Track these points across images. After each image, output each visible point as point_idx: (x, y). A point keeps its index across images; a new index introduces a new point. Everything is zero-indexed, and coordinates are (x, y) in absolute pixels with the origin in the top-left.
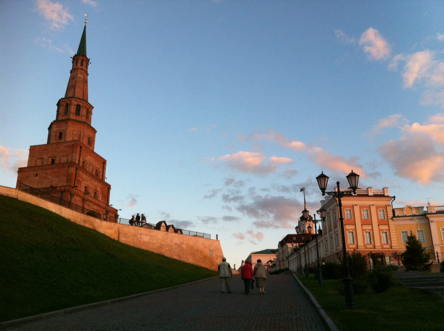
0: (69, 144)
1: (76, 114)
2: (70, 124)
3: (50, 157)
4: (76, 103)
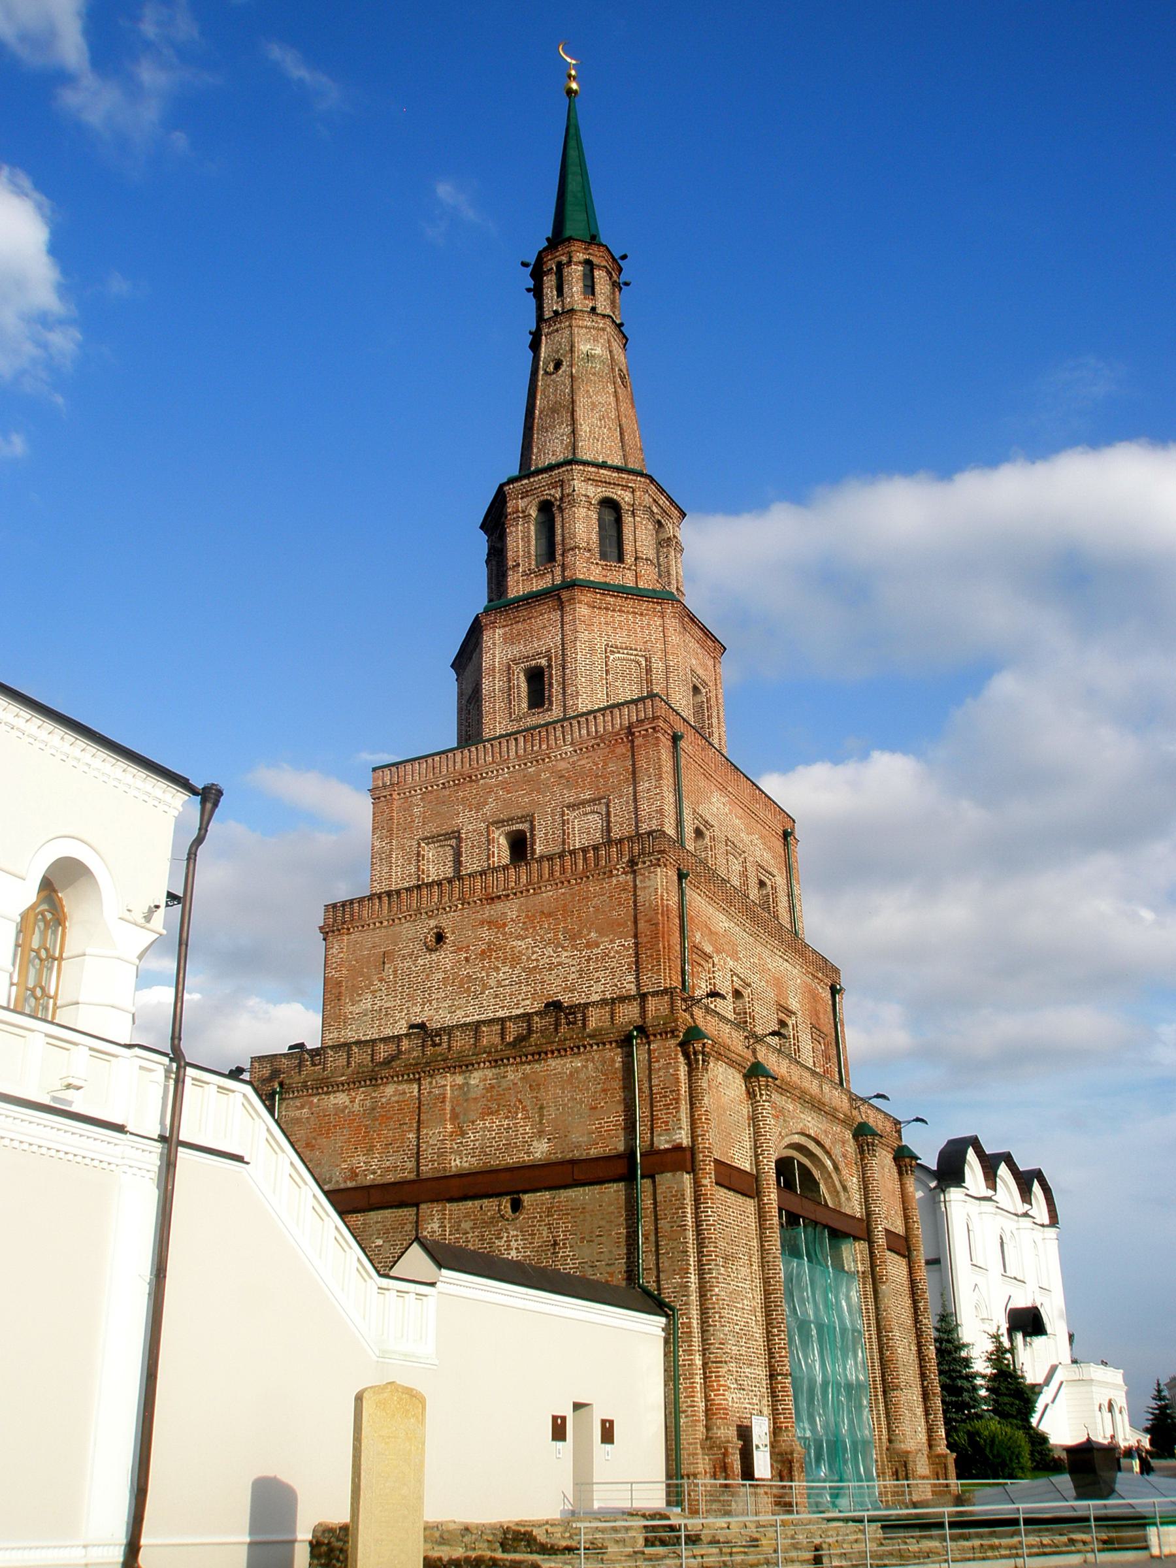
0: (602, 724)
1: (603, 556)
2: (583, 610)
3: (499, 823)
4: (596, 493)
